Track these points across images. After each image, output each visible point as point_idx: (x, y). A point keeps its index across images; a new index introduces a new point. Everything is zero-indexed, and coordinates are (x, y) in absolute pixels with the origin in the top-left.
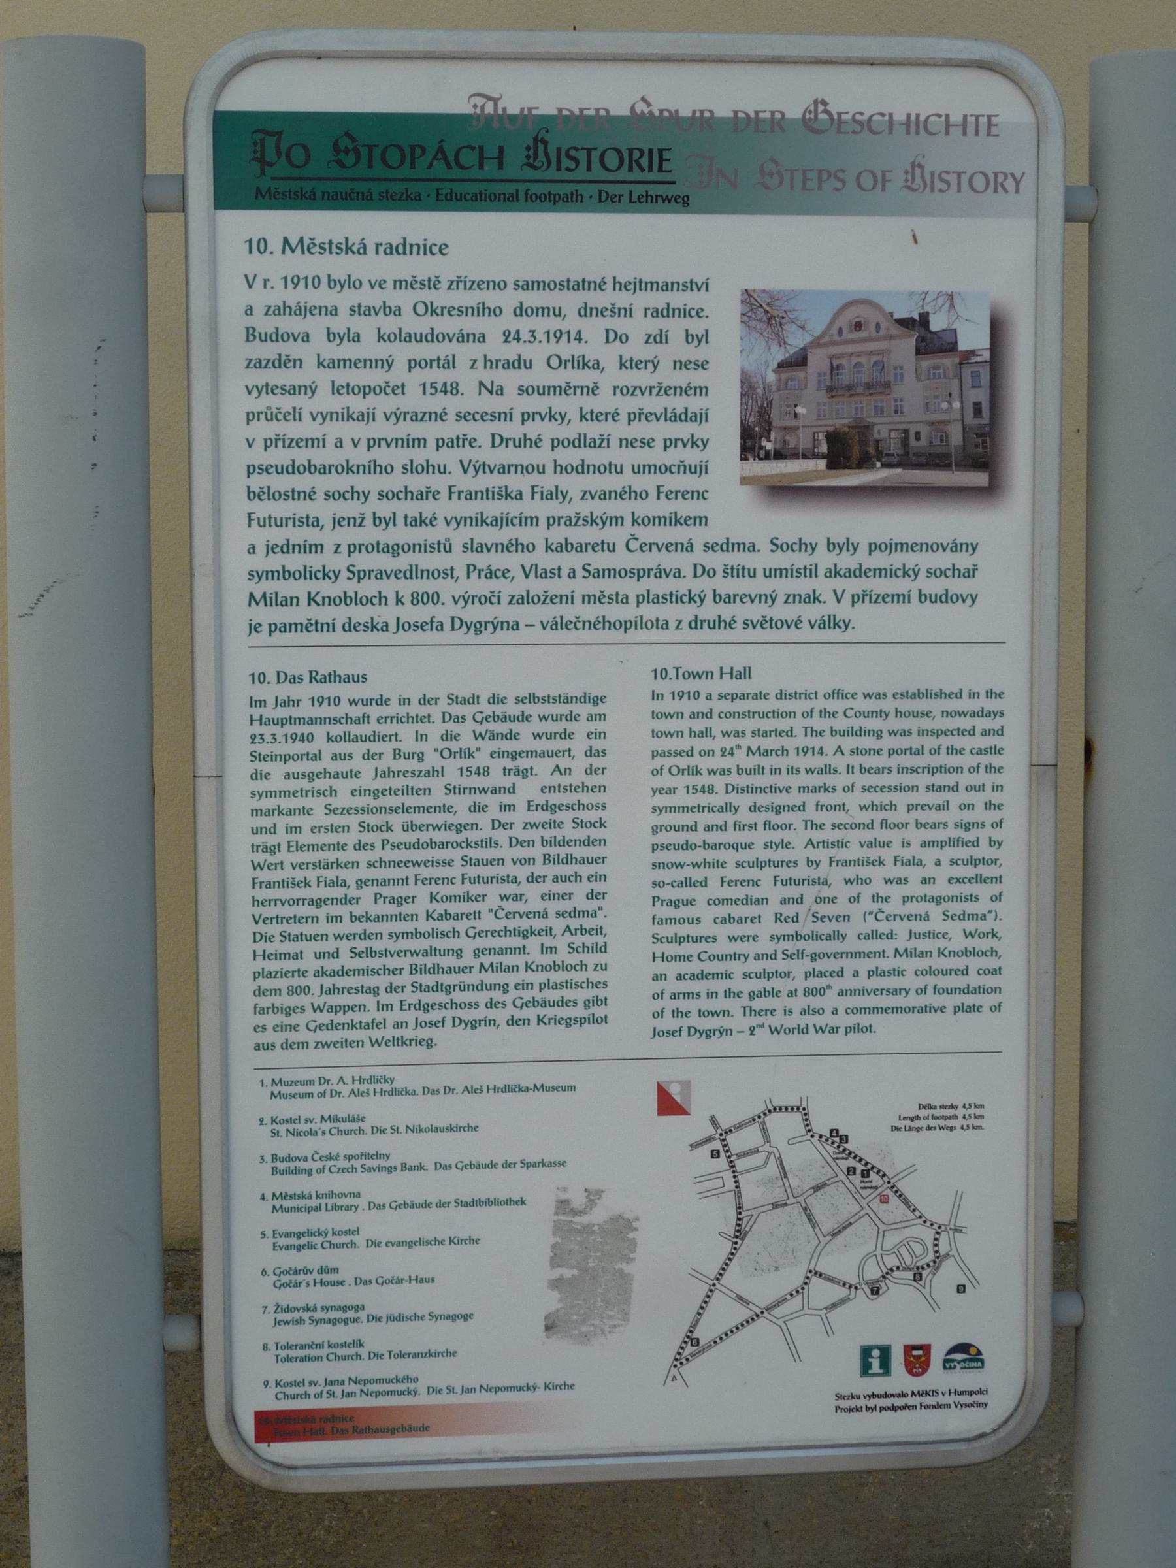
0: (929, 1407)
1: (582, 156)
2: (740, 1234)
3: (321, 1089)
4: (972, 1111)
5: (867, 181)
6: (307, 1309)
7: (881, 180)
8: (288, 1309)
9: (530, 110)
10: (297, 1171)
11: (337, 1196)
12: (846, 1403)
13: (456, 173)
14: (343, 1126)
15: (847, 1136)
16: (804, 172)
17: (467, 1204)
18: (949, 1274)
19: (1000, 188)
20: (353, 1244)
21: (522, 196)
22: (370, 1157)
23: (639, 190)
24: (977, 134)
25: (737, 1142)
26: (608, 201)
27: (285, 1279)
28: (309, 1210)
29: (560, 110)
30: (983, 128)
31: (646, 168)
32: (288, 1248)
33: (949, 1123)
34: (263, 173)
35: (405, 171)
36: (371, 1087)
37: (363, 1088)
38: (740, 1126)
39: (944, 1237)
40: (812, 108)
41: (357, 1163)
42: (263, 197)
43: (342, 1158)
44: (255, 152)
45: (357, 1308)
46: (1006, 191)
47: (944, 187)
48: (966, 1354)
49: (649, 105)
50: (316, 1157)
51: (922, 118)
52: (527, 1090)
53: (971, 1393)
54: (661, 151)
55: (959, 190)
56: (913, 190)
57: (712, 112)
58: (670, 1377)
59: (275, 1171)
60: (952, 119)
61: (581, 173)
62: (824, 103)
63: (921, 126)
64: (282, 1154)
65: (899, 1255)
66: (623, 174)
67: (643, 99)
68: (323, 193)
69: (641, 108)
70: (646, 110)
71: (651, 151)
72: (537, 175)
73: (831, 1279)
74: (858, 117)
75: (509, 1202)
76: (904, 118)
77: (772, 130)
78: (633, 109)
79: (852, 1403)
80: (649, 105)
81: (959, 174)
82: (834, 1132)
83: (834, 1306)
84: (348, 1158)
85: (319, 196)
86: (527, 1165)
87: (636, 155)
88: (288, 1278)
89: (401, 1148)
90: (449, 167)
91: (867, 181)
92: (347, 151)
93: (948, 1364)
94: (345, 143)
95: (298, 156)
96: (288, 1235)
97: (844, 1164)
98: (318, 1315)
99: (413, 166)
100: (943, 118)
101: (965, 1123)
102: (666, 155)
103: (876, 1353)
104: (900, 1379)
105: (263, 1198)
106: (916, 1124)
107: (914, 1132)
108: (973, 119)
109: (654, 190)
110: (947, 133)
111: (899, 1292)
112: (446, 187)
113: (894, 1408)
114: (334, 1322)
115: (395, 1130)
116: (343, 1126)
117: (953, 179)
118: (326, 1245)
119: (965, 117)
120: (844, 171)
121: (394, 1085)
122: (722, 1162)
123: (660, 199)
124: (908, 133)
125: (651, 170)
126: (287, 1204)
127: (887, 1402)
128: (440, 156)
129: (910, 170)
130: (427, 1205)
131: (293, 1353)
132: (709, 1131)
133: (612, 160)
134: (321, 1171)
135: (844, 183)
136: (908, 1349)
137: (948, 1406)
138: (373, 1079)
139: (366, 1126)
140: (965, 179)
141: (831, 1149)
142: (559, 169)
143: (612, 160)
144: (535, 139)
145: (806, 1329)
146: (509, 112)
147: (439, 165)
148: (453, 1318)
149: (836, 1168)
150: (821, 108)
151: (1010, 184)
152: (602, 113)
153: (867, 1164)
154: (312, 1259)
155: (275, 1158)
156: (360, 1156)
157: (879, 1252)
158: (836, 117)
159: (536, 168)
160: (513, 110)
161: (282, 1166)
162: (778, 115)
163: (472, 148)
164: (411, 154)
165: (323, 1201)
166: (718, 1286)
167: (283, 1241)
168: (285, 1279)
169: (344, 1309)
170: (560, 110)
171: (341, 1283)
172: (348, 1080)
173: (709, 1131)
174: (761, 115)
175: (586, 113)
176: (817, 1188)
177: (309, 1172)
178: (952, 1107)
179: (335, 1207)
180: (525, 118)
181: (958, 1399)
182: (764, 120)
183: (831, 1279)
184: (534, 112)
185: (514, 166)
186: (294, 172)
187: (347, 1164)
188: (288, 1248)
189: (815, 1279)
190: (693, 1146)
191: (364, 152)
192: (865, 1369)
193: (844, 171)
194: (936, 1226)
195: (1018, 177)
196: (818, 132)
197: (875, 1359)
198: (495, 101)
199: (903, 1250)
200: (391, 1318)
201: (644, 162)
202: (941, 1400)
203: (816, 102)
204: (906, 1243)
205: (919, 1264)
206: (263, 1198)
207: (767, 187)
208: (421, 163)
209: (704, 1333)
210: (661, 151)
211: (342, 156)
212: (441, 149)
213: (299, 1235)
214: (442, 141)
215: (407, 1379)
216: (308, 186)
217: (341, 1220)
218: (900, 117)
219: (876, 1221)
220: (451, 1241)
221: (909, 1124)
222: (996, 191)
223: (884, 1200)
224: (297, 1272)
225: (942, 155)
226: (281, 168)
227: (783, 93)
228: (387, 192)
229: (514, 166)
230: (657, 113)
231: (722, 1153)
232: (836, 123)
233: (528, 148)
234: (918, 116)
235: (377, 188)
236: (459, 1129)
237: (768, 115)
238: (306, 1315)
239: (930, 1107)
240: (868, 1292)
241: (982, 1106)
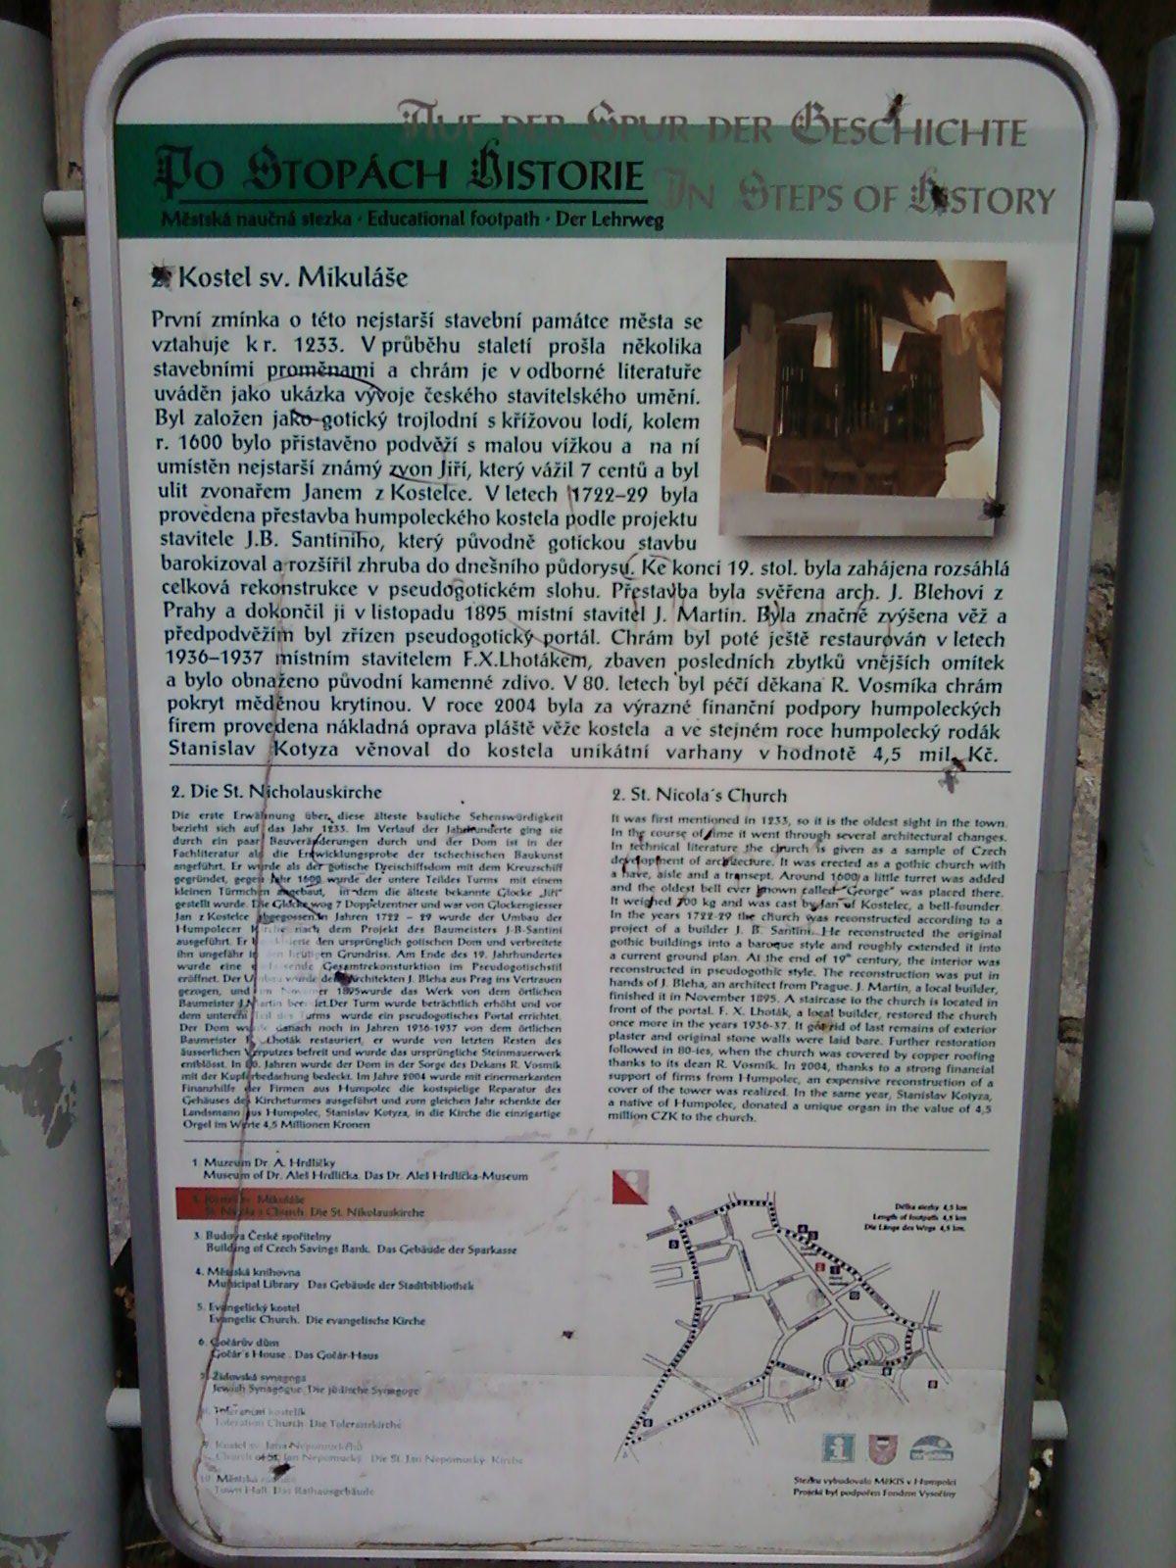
0: (893, 1494)
1: (538, 171)
2: (698, 1323)
3: (258, 1170)
4: (954, 1213)
5: (868, 198)
9: (470, 118)
11: (276, 1273)
13: (392, 192)
15: (816, 1233)
16: (793, 189)
17: (411, 1287)
19: (1024, 207)
21: (468, 218)
23: (603, 210)
24: (1000, 142)
26: (569, 223)
29: (505, 118)
30: (1007, 138)
31: (613, 184)
33: (928, 1223)
34: (170, 195)
35: (333, 191)
36: (311, 1170)
37: (302, 1170)
38: (701, 1218)
39: (917, 1334)
40: (804, 113)
41: (297, 1244)
42: (171, 222)
43: (280, 1237)
44: (160, 171)
45: (297, 1379)
46: (1031, 211)
47: (959, 206)
49: (610, 110)
50: (253, 1236)
51: (935, 125)
52: (476, 1177)
53: (939, 1483)
54: (630, 165)
55: (976, 210)
56: (922, 210)
57: (684, 119)
58: (621, 1454)
59: (210, 1247)
60: (971, 126)
61: (537, 190)
62: (818, 107)
63: (933, 132)
65: (868, 1351)
66: (586, 192)
67: (603, 104)
68: (239, 217)
69: (600, 114)
70: (607, 117)
71: (618, 165)
74: (858, 124)
75: (456, 1286)
76: (914, 125)
77: (757, 136)
78: (591, 114)
79: (813, 1487)
80: (610, 110)
81: (977, 191)
85: (234, 220)
87: (601, 169)
90: (383, 185)
91: (868, 198)
92: (265, 169)
94: (261, 159)
95: (209, 174)
98: (257, 1383)
99: (341, 186)
100: (960, 125)
101: (945, 1224)
102: (636, 169)
103: (839, 1442)
104: (863, 1466)
105: (198, 1272)
106: (892, 1223)
107: (889, 1231)
108: (996, 125)
109: (622, 210)
110: (964, 142)
113: (856, 1493)
117: (969, 196)
118: (265, 1319)
119: (986, 122)
120: (840, 188)
121: (335, 1169)
123: (628, 221)
124: (918, 142)
125: (618, 186)
128: (372, 173)
129: (918, 185)
130: (369, 1286)
132: (669, 1221)
133: (573, 175)
135: (840, 201)
137: (913, 1494)
138: (311, 1162)
140: (983, 196)
141: (799, 1245)
142: (510, 186)
143: (573, 175)
144: (483, 152)
146: (446, 120)
147: (372, 185)
149: (807, 1268)
150: (814, 113)
151: (1037, 202)
152: (555, 121)
153: (837, 1260)
156: (299, 1237)
157: (846, 1347)
158: (832, 124)
159: (483, 185)
162: (763, 123)
163: (410, 163)
164: (338, 172)
165: (262, 1279)
166: (674, 1372)
169: (286, 1379)
170: (505, 118)
171: (282, 1355)
172: (286, 1162)
173: (669, 1221)
174: (743, 122)
175: (535, 121)
176: (782, 1282)
178: (931, 1207)
179: (274, 1284)
180: (467, 128)
181: (924, 1488)
182: (747, 128)
184: (475, 121)
185: (459, 182)
186: (203, 194)
187: (285, 1244)
189: (777, 1370)
190: (650, 1236)
191: (285, 171)
192: (829, 1454)
193: (840, 188)
194: (909, 1324)
195: (1047, 195)
196: (814, 141)
199: (872, 1345)
201: (611, 178)
202: (906, 1488)
203: (808, 106)
204: (876, 1339)
205: (889, 1359)
206: (198, 1272)
207: (748, 206)
208: (351, 182)
210: (630, 165)
211: (260, 175)
212: (373, 164)
214: (374, 155)
219: (846, 1316)
220: (395, 1321)
221: (884, 1223)
222: (1019, 210)
223: (855, 1296)
224: (235, 1343)
226: (191, 190)
227: (769, 95)
228: (312, 215)
229: (459, 182)
230: (619, 121)
231: (681, 1244)
232: (832, 133)
233: (475, 163)
234: (930, 122)
235: (300, 211)
237: (751, 122)
238: (246, 1383)
239: (908, 1207)
240: (834, 1384)
241: (965, 1208)
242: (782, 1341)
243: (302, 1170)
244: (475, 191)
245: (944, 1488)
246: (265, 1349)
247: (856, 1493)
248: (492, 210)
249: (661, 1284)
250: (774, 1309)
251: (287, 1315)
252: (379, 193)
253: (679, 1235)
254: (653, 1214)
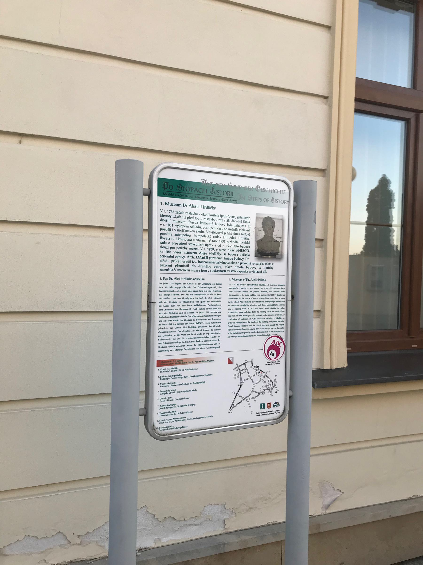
1: (220, 192)
2: (241, 385)
5: (265, 200)
6: (166, 405)
7: (267, 200)
8: (162, 406)
10: (165, 379)
12: (258, 414)
13: (199, 193)
14: (174, 370)
18: (274, 390)
20: (175, 392)
22: (178, 375)
23: (229, 199)
25: (241, 368)
27: (162, 400)
28: (167, 386)
32: (163, 394)
38: (241, 365)
41: (176, 377)
48: (277, 404)
59: (161, 379)
61: (219, 195)
64: (162, 376)
65: (267, 387)
66: (226, 196)
69: (230, 184)
72: (213, 195)
73: (256, 392)
75: (202, 382)
79: (259, 414)
82: (257, 365)
83: (256, 397)
84: (174, 376)
86: (206, 375)
88: (162, 400)
89: (184, 373)
91: (265, 200)
93: (274, 406)
95: (171, 187)
96: (163, 391)
97: (258, 371)
98: (168, 407)
104: (267, 409)
109: (232, 199)
111: (267, 394)
112: (197, 195)
113: (265, 415)
114: (171, 408)
115: (183, 370)
116: (174, 370)
117: (278, 201)
122: (238, 372)
126: (163, 385)
127: (264, 414)
131: (163, 414)
132: (236, 366)
133: (225, 193)
134: (169, 379)
136: (268, 404)
139: (178, 370)
143: (225, 193)
145: (252, 401)
148: (192, 405)
154: (167, 396)
155: (161, 377)
160: (209, 183)
161: (162, 378)
167: (162, 393)
168: (162, 400)
169: (173, 405)
173: (236, 366)
176: (254, 376)
177: (167, 379)
179: (172, 385)
180: (211, 184)
183: (256, 392)
186: (170, 190)
188: (163, 394)
189: (253, 392)
190: (234, 369)
192: (261, 408)
197: (262, 406)
198: (206, 181)
200: (181, 406)
201: (230, 194)
202: (273, 412)
204: (268, 385)
208: (193, 191)
209: (235, 404)
213: (165, 391)
215: (184, 417)
216: (173, 193)
217: (173, 388)
218: (271, 190)
219: (263, 381)
223: (264, 377)
224: (164, 399)
225: (277, 197)
226: (168, 189)
236: (194, 369)
238: (165, 407)
242: (254, 387)
243: (177, 362)
244: (211, 194)
245: (277, 412)
246: (170, 399)
247: (265, 415)
248: (214, 197)
249: (235, 378)
250: (252, 381)
251: (173, 391)
252: (197, 193)
253: (238, 368)
254: (234, 365)
